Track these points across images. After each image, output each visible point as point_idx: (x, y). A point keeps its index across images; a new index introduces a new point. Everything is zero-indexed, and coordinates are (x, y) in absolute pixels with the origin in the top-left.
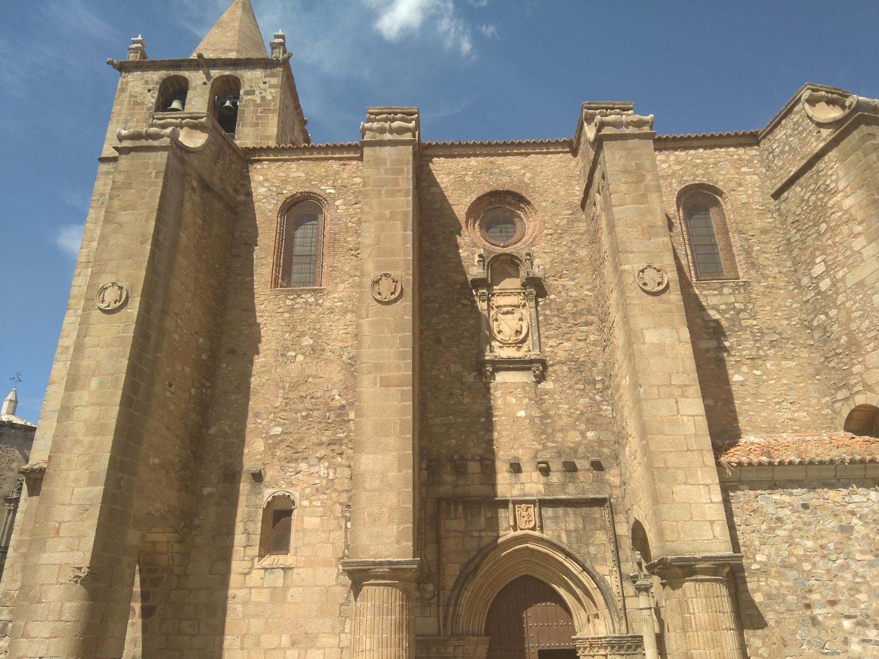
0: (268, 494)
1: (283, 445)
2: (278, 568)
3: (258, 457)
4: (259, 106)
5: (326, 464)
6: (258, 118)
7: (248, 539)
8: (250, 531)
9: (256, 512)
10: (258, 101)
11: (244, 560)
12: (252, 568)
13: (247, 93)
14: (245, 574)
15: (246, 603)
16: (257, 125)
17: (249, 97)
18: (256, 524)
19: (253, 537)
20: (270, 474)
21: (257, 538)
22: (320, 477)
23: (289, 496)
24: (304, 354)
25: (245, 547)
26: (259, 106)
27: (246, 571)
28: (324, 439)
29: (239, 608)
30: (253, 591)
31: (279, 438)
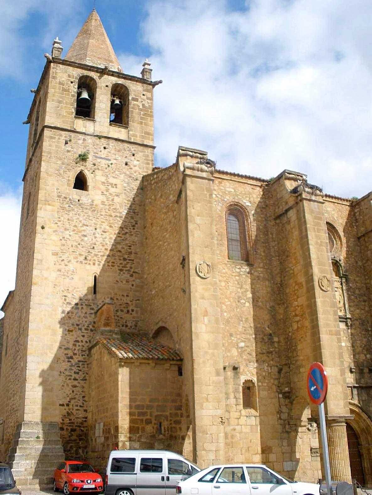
0: (243, 379)
1: (246, 353)
2: (252, 416)
3: (235, 358)
4: (141, 110)
5: (267, 364)
6: (142, 118)
7: (237, 401)
8: (237, 397)
9: (239, 387)
10: (141, 107)
11: (236, 412)
12: (241, 415)
13: (134, 99)
14: (238, 419)
15: (241, 433)
16: (141, 123)
17: (135, 103)
18: (239, 393)
19: (239, 400)
20: (242, 368)
21: (241, 401)
22: (265, 371)
23: (252, 380)
24: (249, 302)
25: (236, 405)
26: (141, 110)
27: (238, 417)
28: (264, 351)
29: (238, 435)
30: (243, 427)
31: (244, 349)
